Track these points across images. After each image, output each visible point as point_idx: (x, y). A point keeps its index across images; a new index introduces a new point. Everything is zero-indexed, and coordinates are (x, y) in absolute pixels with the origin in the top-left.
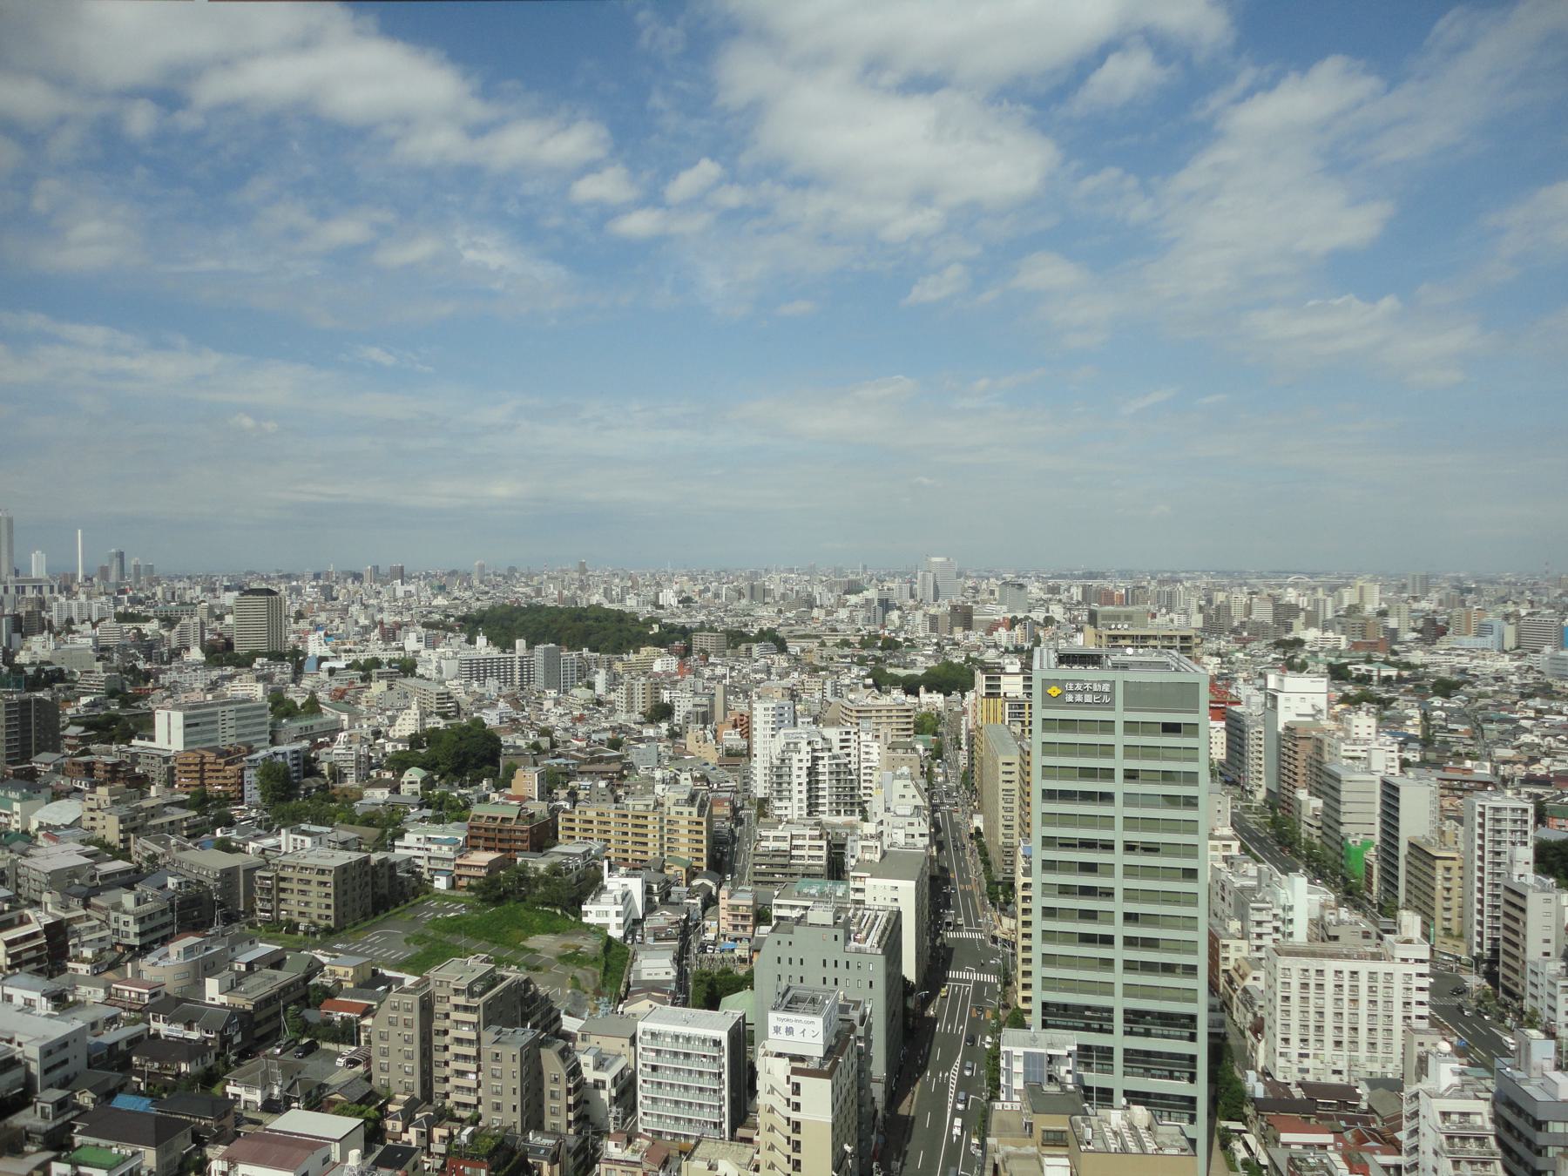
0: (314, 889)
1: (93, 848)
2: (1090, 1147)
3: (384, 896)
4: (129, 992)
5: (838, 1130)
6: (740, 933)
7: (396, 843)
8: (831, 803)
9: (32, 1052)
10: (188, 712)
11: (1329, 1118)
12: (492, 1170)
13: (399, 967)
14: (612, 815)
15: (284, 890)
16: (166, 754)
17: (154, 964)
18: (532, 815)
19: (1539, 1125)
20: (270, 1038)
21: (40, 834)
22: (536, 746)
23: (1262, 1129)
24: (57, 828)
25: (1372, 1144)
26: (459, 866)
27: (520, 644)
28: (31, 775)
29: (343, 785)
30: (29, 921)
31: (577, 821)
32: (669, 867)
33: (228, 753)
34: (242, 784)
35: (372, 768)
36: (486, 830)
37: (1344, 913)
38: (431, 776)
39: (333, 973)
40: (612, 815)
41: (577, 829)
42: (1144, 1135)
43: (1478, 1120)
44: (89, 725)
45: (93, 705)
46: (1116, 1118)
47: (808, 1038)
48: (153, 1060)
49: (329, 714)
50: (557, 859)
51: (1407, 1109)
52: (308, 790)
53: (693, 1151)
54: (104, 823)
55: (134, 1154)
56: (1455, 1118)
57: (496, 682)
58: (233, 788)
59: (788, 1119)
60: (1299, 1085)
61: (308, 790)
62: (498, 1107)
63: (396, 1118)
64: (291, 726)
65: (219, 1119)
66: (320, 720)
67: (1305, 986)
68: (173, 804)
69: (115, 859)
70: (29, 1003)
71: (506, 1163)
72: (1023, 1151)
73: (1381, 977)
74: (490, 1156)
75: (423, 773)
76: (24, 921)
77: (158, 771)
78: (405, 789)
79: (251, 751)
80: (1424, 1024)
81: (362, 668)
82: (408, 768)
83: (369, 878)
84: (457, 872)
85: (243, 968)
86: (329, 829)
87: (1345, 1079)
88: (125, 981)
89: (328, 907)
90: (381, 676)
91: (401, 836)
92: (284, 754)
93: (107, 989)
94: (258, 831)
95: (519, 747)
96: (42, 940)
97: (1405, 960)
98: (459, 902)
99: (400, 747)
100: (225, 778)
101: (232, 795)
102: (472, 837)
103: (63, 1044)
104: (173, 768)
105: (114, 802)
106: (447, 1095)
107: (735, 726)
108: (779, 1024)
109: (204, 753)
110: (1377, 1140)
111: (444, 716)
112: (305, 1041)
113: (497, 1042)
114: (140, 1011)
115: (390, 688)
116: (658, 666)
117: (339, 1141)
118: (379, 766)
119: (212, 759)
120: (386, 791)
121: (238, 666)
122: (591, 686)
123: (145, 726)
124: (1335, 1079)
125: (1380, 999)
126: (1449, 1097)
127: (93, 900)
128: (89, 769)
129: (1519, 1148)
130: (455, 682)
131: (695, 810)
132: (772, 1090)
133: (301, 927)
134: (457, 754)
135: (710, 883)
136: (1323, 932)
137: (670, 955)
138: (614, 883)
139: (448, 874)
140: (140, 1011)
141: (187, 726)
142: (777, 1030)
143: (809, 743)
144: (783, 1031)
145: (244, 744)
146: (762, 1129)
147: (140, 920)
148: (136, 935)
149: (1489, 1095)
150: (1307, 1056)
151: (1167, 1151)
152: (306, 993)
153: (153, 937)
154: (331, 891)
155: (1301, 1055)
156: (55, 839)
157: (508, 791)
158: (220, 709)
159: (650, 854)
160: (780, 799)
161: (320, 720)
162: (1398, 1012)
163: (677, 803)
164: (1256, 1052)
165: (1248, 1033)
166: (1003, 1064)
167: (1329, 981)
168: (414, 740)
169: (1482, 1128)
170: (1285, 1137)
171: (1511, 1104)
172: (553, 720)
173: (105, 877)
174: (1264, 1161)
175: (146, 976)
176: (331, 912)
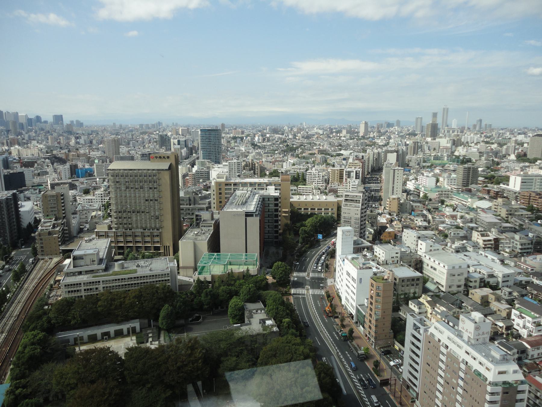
4: (524, 266)
9: (500, 275)
10: (523, 178)
21: (479, 210)
28: (470, 191)
30: (489, 236)
44: (486, 178)
45: (483, 171)
54: (500, 210)
55: (539, 317)
68: (521, 208)
88: (520, 262)
93: (516, 263)
96: (493, 242)
100: (538, 203)
101: (540, 209)
104: (517, 196)
105: (504, 204)
109: (531, 193)
114: (527, 273)
119: (534, 195)
121: (530, 163)
140: (527, 273)
141: (522, 182)
147: (522, 245)
156: (485, 212)
158: (534, 178)
175: (527, 263)
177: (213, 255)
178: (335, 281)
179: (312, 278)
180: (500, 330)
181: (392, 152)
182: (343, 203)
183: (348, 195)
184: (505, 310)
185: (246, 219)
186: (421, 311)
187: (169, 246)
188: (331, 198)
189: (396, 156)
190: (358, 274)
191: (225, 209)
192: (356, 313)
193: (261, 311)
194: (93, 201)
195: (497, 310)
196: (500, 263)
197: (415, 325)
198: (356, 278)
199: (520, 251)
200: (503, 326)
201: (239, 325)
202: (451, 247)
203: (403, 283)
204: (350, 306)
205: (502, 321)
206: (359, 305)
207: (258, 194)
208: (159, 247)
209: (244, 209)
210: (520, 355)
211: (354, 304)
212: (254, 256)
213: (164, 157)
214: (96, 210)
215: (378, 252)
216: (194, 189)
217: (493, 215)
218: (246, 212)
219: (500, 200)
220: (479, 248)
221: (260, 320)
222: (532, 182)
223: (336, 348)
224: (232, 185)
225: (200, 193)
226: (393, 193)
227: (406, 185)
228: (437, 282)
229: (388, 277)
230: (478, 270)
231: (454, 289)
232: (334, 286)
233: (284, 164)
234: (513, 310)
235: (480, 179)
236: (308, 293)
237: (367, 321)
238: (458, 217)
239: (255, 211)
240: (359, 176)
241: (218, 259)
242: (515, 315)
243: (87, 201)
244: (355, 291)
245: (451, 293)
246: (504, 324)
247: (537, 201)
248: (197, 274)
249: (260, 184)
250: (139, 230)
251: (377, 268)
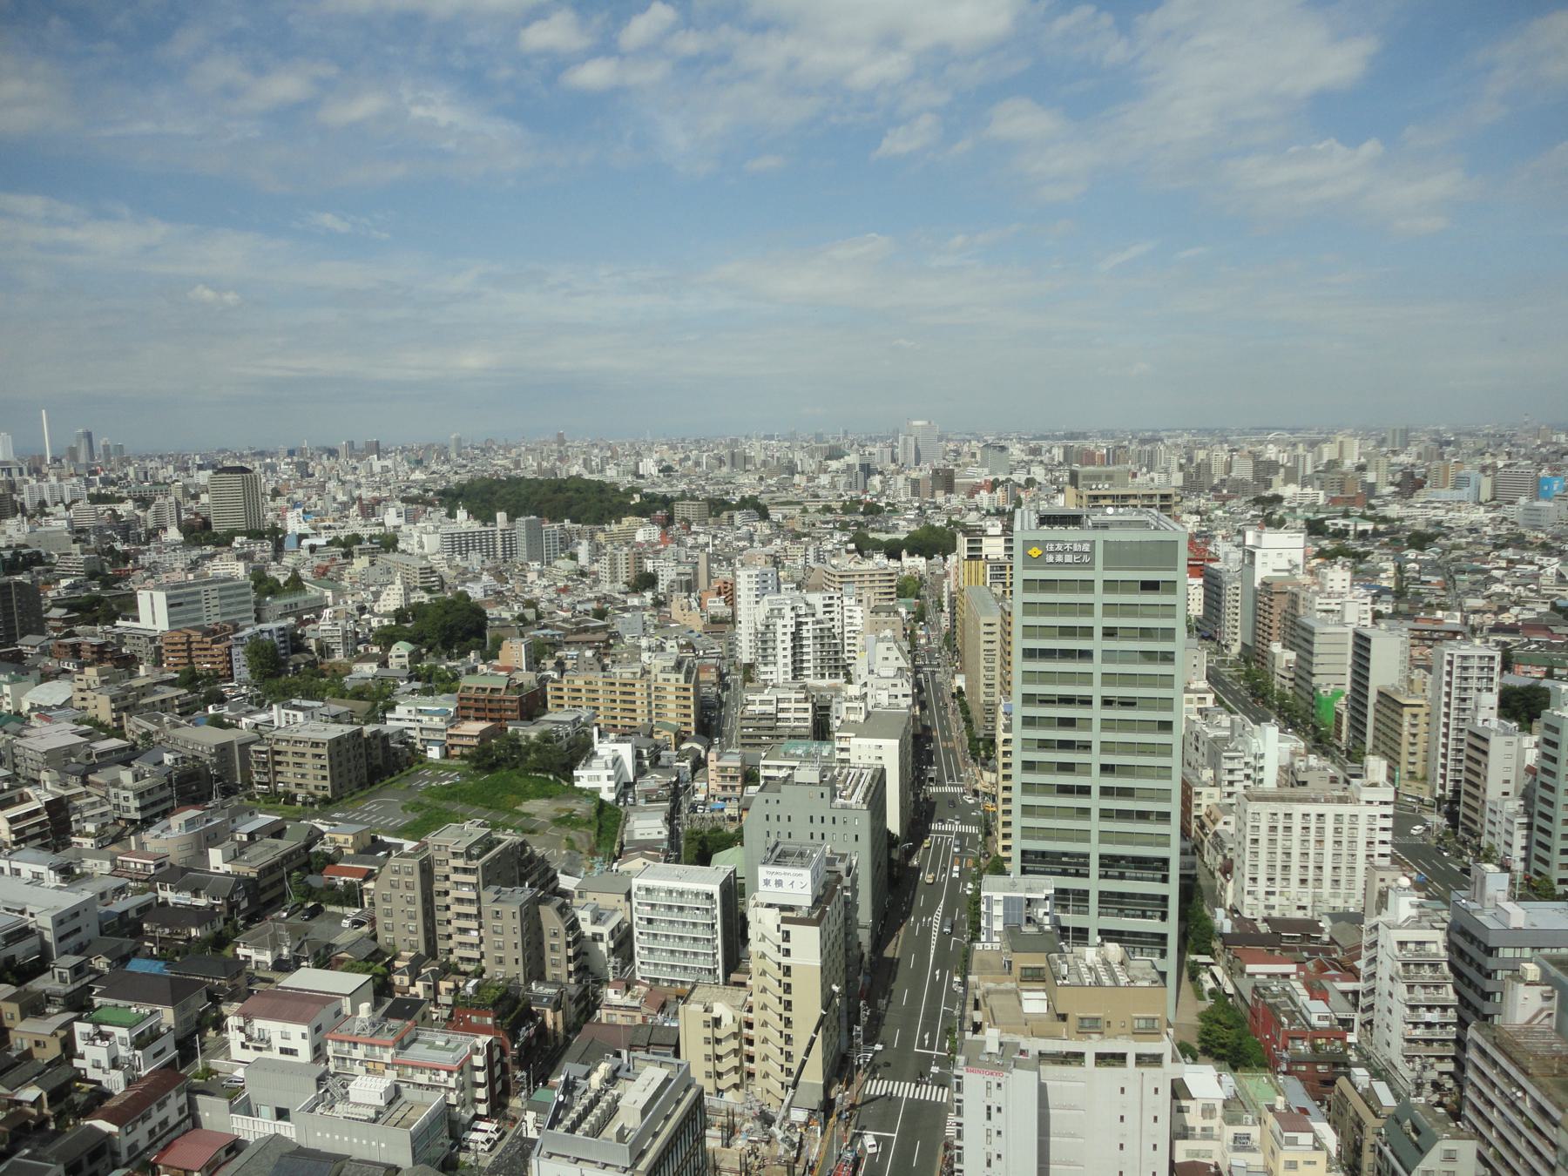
0: (309, 760)
1: (86, 727)
2: (1066, 982)
3: (378, 767)
4: (136, 863)
5: (826, 973)
6: (729, 793)
8: (815, 667)
9: (45, 921)
10: (170, 592)
11: (1293, 950)
12: (498, 1018)
13: (398, 833)
14: (600, 684)
15: (279, 763)
16: (152, 634)
17: (157, 837)
18: (521, 685)
19: (1490, 951)
20: (276, 902)
21: (33, 715)
22: (521, 618)
23: (1229, 961)
24: (49, 709)
25: (1333, 972)
26: (450, 736)
27: (501, 516)
28: (18, 658)
29: (331, 661)
30: (29, 799)
31: (565, 690)
32: (658, 732)
33: (214, 632)
34: (230, 662)
35: (359, 643)
36: (476, 700)
37: (1313, 760)
38: (419, 650)
39: (333, 840)
40: (600, 684)
41: (566, 698)
42: (1117, 969)
43: (1433, 948)
44: (72, 607)
46: (1090, 954)
47: (797, 889)
48: (163, 926)
49: (313, 591)
50: (547, 727)
51: (1366, 939)
52: (296, 666)
53: (689, 995)
54: (94, 702)
55: (152, 1013)
56: (1411, 946)
57: (479, 556)
58: (221, 666)
59: (779, 964)
60: (1265, 920)
61: (296, 666)
62: (500, 961)
63: (403, 973)
64: (275, 604)
65: (232, 978)
67: (1273, 829)
68: (163, 683)
69: (109, 737)
70: (37, 877)
71: (511, 1011)
72: (1002, 987)
73: (1346, 819)
74: (495, 1004)
75: (410, 647)
76: (24, 799)
77: (145, 651)
78: (394, 663)
79: (237, 629)
80: (1386, 862)
81: (343, 545)
82: (395, 642)
83: (363, 750)
84: (450, 741)
85: (245, 838)
86: (321, 704)
87: (1309, 914)
88: (130, 853)
89: (324, 778)
90: (362, 552)
91: (392, 708)
92: (270, 632)
93: (113, 861)
94: (250, 707)
95: (505, 619)
96: (45, 817)
97: (1370, 803)
98: (453, 771)
99: (386, 622)
100: (213, 656)
101: (221, 673)
102: (462, 708)
103: (75, 913)
104: (160, 647)
106: (451, 951)
107: (719, 594)
108: (769, 877)
109: (190, 632)
110: (1336, 968)
111: (429, 590)
112: (310, 904)
113: (496, 901)
114: (146, 881)
115: (372, 563)
116: (640, 536)
117: (349, 995)
118: (366, 641)
119: (199, 638)
120: (375, 665)
121: (218, 545)
122: (574, 557)
123: (128, 606)
124: (1299, 915)
125: (1345, 840)
126: (1407, 928)
127: (91, 777)
128: (75, 651)
129: (1470, 972)
130: (438, 557)
131: (682, 677)
132: (763, 938)
133: (299, 798)
134: (444, 628)
135: (697, 746)
136: (1292, 778)
137: (662, 815)
138: (604, 748)
139: (441, 744)
140: (146, 881)
141: (170, 606)
142: (767, 882)
143: (793, 609)
144: (772, 883)
145: (229, 622)
146: (754, 973)
147: (140, 795)
148: (137, 809)
149: (1445, 925)
150: (1273, 893)
151: (1139, 984)
152: (308, 860)
153: (154, 811)
154: (326, 762)
155: (1268, 893)
156: (49, 719)
157: (496, 663)
158: (206, 588)
159: (639, 720)
160: (766, 664)
161: (303, 598)
162: (1361, 852)
163: (663, 670)
164: (1225, 891)
165: (1218, 874)
166: (983, 908)
167: (1297, 824)
168: (400, 615)
169: (1436, 955)
170: (1250, 968)
171: (1464, 933)
172: (537, 592)
173: (101, 755)
174: (1230, 990)
175: (150, 848)
176: (327, 783)
180: (34, 1111)
184: (54, 1034)
200: (41, 1096)
205: (35, 1083)
217: (74, 721)
222: (199, 601)
234: (76, 1024)
246: (42, 1088)
247: (209, 652)
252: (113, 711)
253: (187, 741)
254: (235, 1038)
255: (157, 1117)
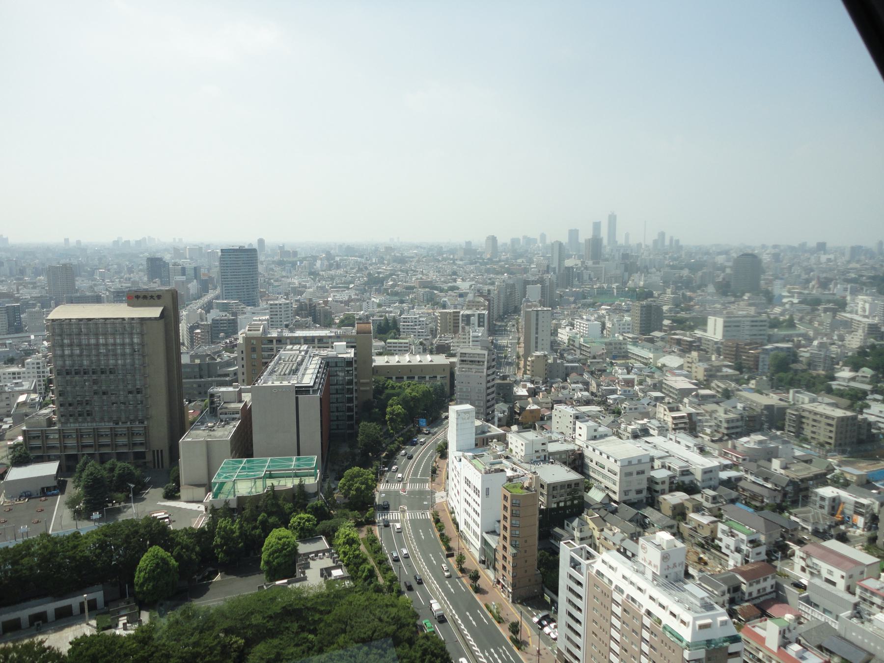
7: (865, 411)
16: (716, 340)
44: (674, 321)
45: (670, 310)
49: (801, 328)
54: (696, 370)
66: (797, 332)
76: (678, 410)
79: (762, 344)
89: (830, 438)
90: (826, 310)
91: (868, 407)
100: (748, 357)
121: (735, 296)
141: (725, 327)
168: (862, 352)
177: (241, 462)
178: (448, 494)
179: (411, 493)
181: (534, 283)
182: (458, 366)
183: (465, 354)
184: (708, 525)
185: (297, 398)
186: (584, 535)
187: (162, 451)
188: (441, 359)
189: (540, 290)
190: (483, 481)
191: (260, 383)
192: (482, 546)
193: (324, 555)
194: (22, 375)
195: (697, 526)
196: (698, 451)
197: (572, 559)
198: (479, 488)
199: (725, 432)
201: (285, 581)
202: (625, 430)
203: (555, 492)
204: (472, 535)
206: (487, 533)
207: (317, 355)
208: (144, 453)
209: (294, 381)
210: (733, 595)
211: (478, 531)
212: (312, 460)
213: (152, 297)
214: (28, 392)
215: (515, 444)
216: (209, 349)
218: (296, 387)
219: (694, 354)
220: (667, 430)
221: (322, 570)
223: (451, 607)
224: (275, 341)
225: (219, 356)
226: (536, 347)
227: (557, 335)
228: (606, 487)
229: (530, 484)
230: (667, 464)
231: (633, 497)
232: (447, 503)
233: (364, 304)
235: (666, 322)
236: (404, 517)
237: (499, 556)
238: (636, 383)
239: (312, 384)
240: (483, 322)
241: (249, 468)
242: (723, 532)
243: (11, 376)
244: (479, 510)
245: (628, 502)
248: (211, 496)
249: (321, 339)
250: (107, 424)
251: (513, 469)
252: (705, 376)
253: (747, 399)
254: (798, 562)
255: (762, 585)
